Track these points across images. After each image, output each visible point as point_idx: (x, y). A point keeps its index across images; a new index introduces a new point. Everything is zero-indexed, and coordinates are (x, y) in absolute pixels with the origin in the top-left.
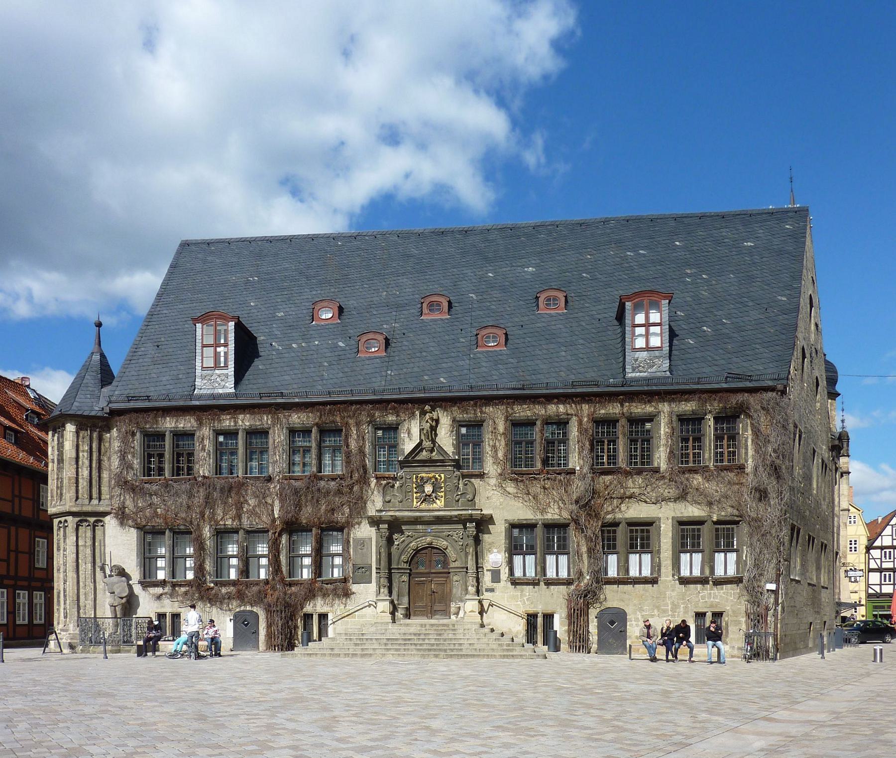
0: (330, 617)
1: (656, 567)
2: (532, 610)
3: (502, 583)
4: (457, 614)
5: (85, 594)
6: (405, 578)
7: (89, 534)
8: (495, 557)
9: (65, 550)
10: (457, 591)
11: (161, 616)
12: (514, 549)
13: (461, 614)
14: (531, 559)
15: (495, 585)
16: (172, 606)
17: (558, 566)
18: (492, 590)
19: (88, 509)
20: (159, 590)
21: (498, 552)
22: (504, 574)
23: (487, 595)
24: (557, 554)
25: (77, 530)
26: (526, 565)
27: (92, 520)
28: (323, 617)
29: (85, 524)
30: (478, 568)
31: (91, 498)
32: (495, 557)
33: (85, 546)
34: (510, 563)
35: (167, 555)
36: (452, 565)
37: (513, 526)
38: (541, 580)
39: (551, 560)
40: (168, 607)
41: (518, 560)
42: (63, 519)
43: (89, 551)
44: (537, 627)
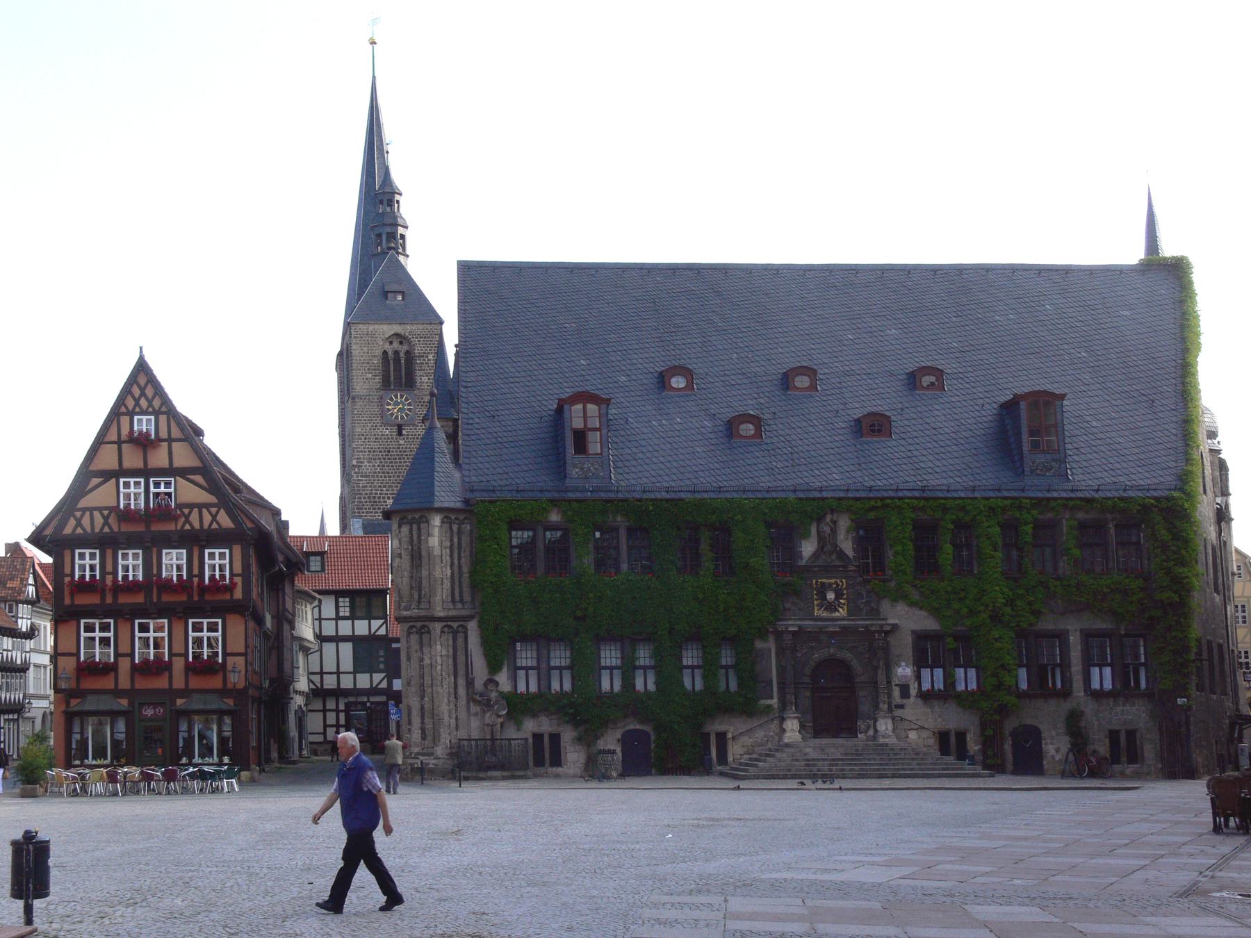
0: (730, 736)
1: (1067, 681)
2: (941, 725)
3: (912, 699)
4: (866, 732)
5: (450, 711)
6: (808, 694)
7: (451, 642)
8: (904, 671)
9: (422, 660)
10: (865, 707)
11: (538, 737)
12: (920, 662)
13: (871, 732)
14: (939, 672)
15: (905, 701)
17: (967, 680)
18: (901, 707)
19: (453, 613)
21: (907, 666)
22: (913, 691)
23: (898, 713)
24: (966, 667)
26: (934, 678)
27: (455, 625)
28: (722, 737)
29: (446, 630)
30: (889, 682)
31: (453, 601)
32: (904, 671)
34: (918, 677)
35: (544, 666)
36: (858, 680)
37: (921, 638)
38: (947, 694)
39: (960, 672)
41: (925, 673)
42: (419, 624)
43: (451, 661)
44: (950, 744)
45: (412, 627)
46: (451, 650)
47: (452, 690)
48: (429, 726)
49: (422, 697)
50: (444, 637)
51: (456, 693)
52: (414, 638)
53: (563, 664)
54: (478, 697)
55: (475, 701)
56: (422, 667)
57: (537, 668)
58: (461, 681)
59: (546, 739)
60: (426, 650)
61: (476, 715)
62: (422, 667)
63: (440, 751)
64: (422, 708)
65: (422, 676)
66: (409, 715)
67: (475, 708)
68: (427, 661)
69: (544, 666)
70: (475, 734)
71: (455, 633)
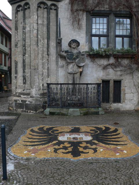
5: (43, 64)
7: (45, 15)
9: (24, 28)
11: (106, 82)
16: (116, 75)
20: (104, 62)
25: (37, 10)
29: (42, 6)
33: (43, 25)
40: (112, 75)
43: (45, 29)
45: (19, 6)
46: (45, 21)
47: (45, 49)
48: (28, 75)
49: (24, 55)
50: (40, 11)
51: (48, 51)
52: (21, 14)
53: (125, 34)
54: (64, 54)
55: (62, 57)
56: (24, 33)
57: (107, 36)
58: (53, 44)
59: (112, 84)
60: (27, 21)
61: (62, 67)
62: (24, 33)
63: (34, 92)
64: (24, 61)
65: (24, 40)
66: (16, 67)
67: (61, 62)
68: (28, 29)
69: (112, 34)
70: (61, 81)
71: (49, 9)
